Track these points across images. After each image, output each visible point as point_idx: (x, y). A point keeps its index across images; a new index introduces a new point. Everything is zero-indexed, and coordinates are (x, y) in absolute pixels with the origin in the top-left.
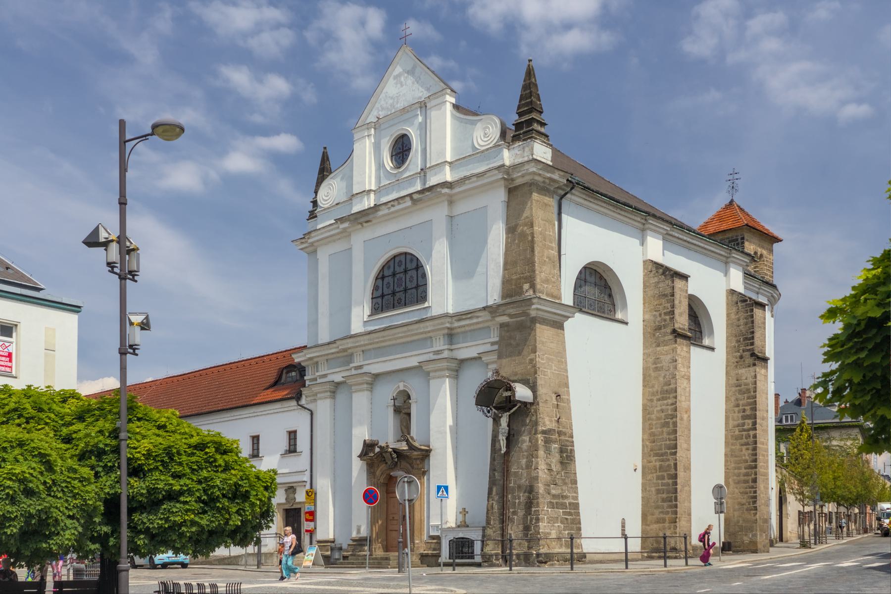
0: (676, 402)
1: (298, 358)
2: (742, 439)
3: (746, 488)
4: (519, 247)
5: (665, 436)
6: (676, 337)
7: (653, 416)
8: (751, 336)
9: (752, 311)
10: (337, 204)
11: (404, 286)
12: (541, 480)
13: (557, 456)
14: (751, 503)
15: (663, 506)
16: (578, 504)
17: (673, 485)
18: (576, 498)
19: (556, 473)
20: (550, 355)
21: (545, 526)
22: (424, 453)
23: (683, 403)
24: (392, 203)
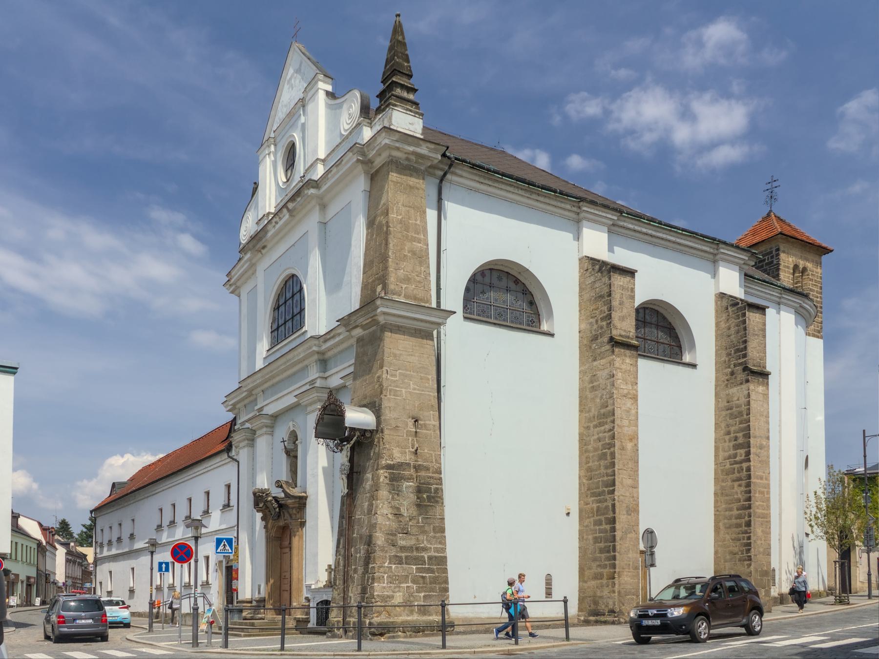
0: (614, 427)
2: (734, 473)
3: (739, 534)
5: (603, 471)
6: (613, 346)
7: (590, 447)
8: (742, 346)
9: (744, 315)
12: (381, 529)
13: (413, 497)
15: (600, 557)
16: (446, 557)
17: (611, 532)
18: (444, 550)
19: (408, 519)
20: (407, 370)
21: (384, 588)
22: (298, 500)
23: (626, 429)
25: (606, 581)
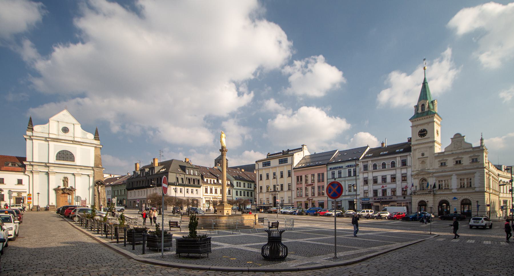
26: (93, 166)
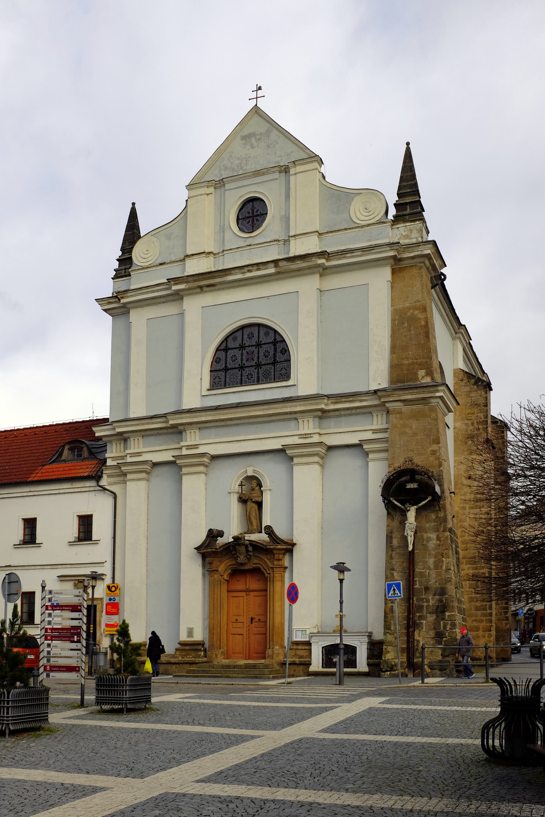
1: (99, 432)
4: (410, 331)
10: (161, 264)
11: (256, 360)
14: (503, 614)
24: (250, 268)
25: (482, 633)
26: (385, 385)
